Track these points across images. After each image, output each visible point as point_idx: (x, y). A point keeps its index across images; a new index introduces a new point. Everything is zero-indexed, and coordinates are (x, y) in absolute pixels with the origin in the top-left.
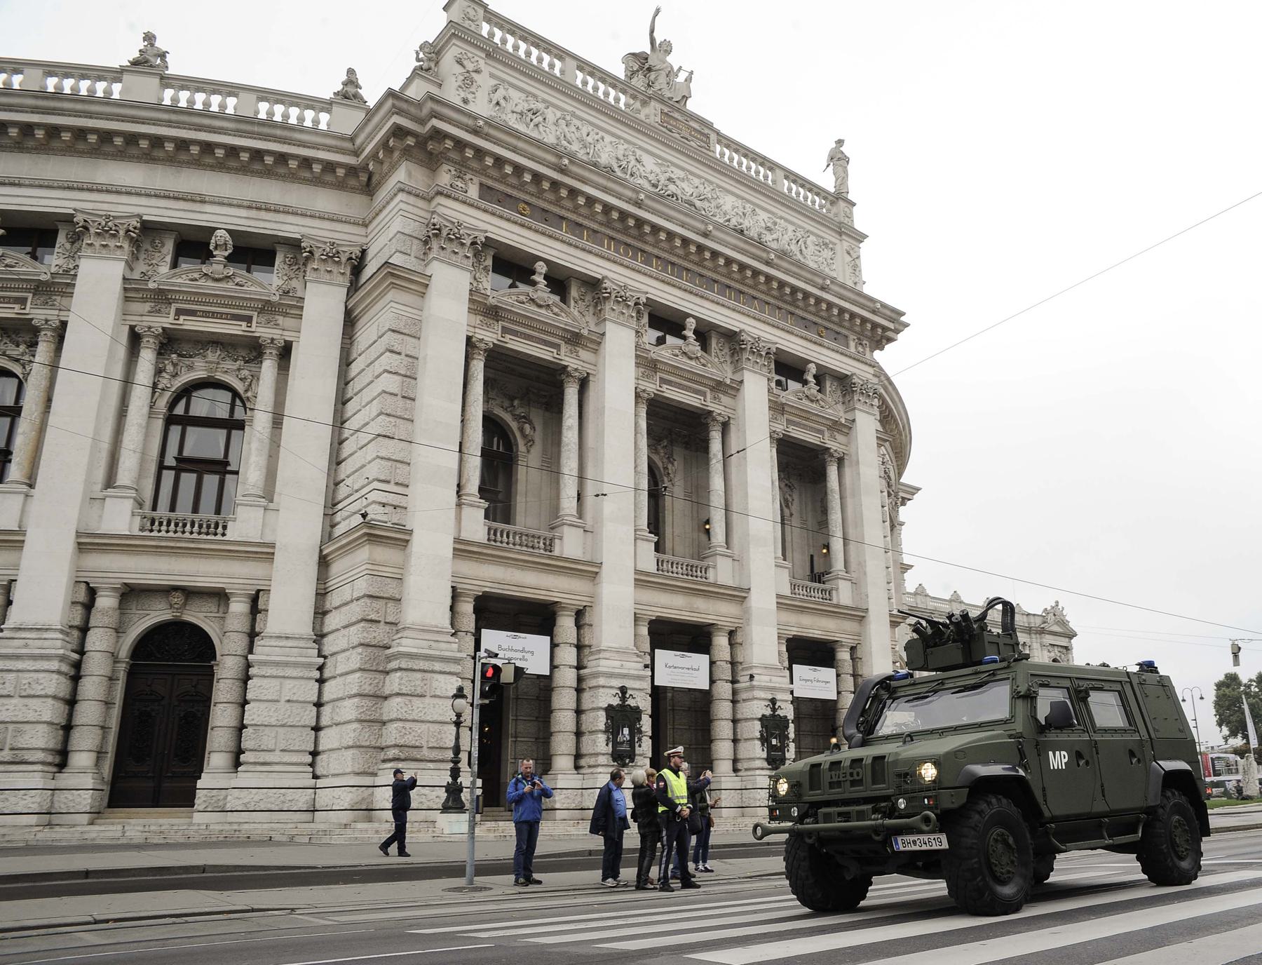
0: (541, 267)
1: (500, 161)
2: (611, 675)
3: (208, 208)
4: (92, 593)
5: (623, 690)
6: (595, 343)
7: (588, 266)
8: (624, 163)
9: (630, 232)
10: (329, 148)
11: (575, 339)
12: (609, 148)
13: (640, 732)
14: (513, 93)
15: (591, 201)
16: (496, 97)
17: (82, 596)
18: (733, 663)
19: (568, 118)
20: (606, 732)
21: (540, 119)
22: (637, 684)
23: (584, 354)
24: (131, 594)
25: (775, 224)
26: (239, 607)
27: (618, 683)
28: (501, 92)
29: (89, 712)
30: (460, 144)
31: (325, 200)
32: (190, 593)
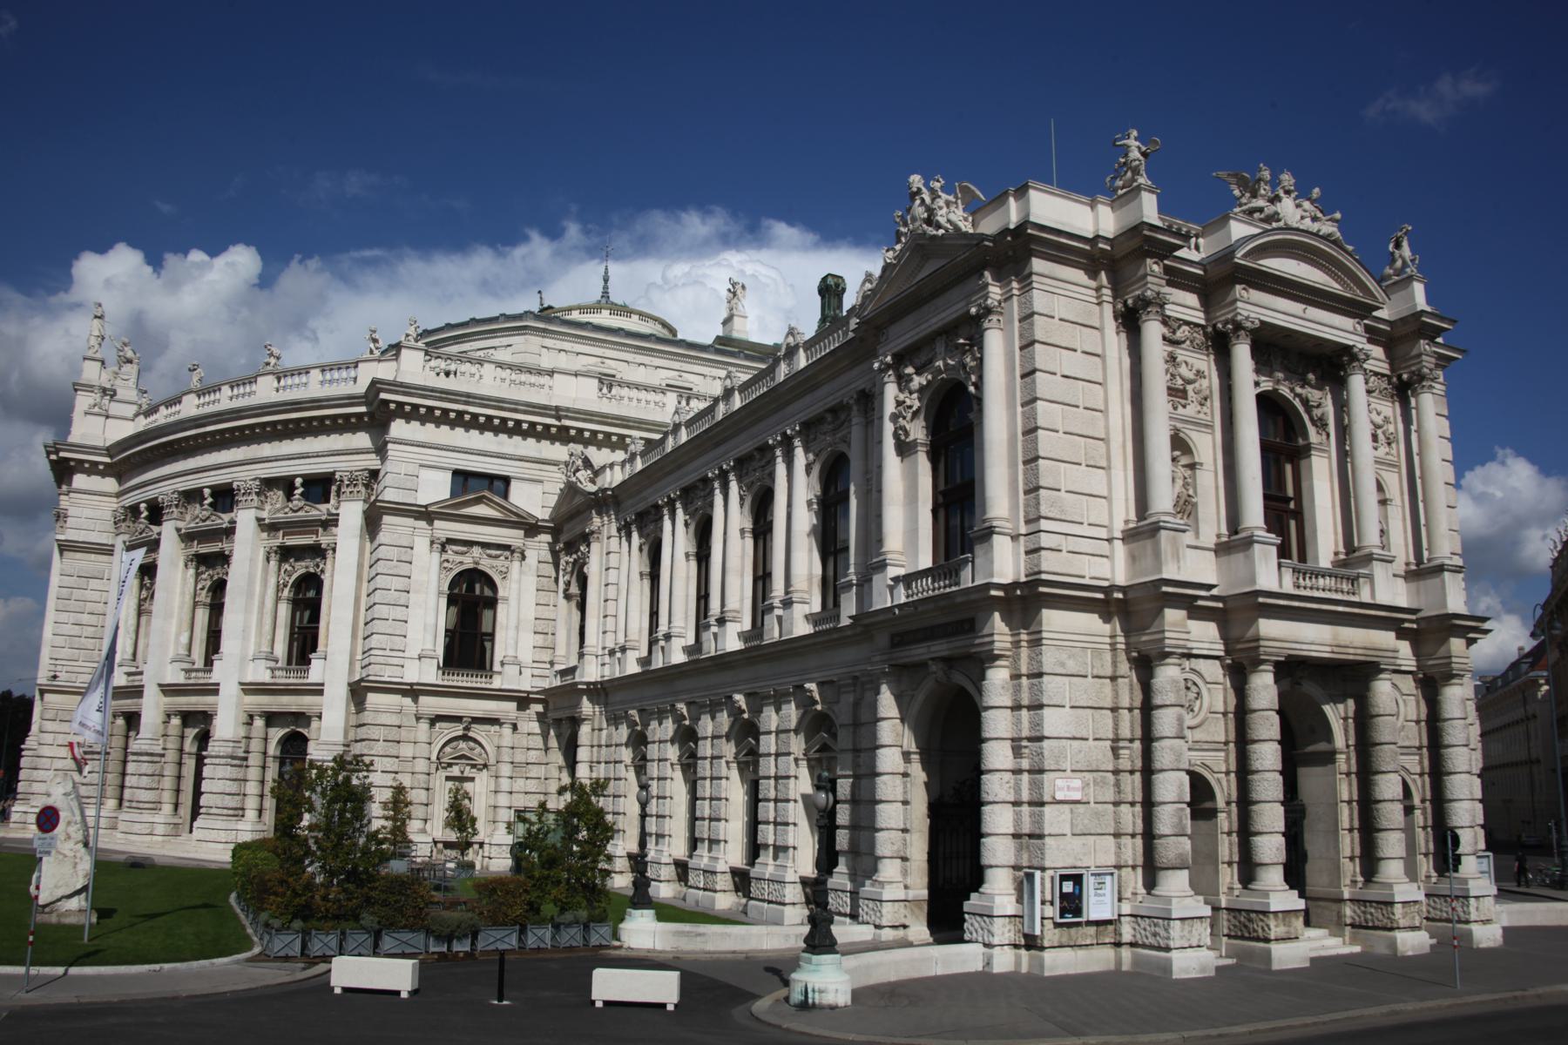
17: (244, 718)
24: (271, 719)
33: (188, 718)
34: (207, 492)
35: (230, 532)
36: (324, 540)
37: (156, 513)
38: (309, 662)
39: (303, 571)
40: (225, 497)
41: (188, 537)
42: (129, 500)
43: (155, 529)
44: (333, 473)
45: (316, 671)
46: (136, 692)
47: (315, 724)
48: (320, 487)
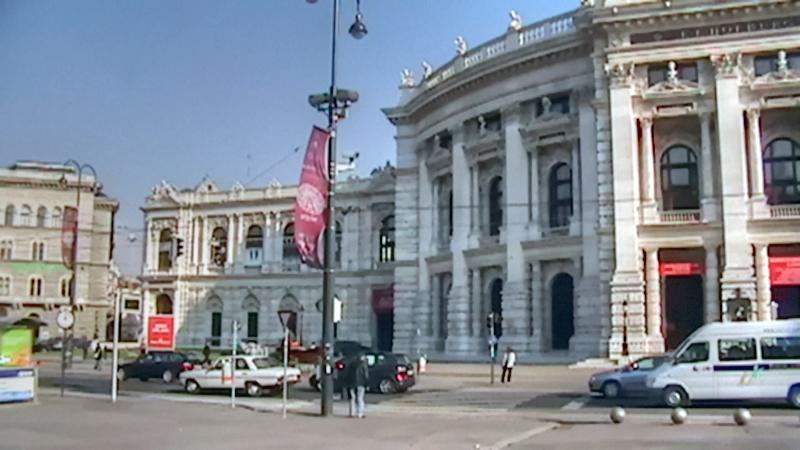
3: (541, 88)
4: (531, 266)
5: (738, 290)
10: (570, 42)
11: (699, 97)
13: (750, 311)
15: (693, 15)
20: (728, 311)
22: (748, 285)
24: (544, 264)
26: (577, 265)
29: (536, 314)
31: (580, 65)
32: (563, 261)
33: (483, 271)
34: (481, 119)
35: (502, 143)
36: (569, 137)
37: (446, 139)
38: (566, 223)
39: (555, 162)
40: (494, 119)
41: (467, 152)
42: (427, 134)
43: (446, 153)
44: (570, 91)
45: (574, 227)
46: (449, 257)
47: (577, 265)
48: (561, 100)
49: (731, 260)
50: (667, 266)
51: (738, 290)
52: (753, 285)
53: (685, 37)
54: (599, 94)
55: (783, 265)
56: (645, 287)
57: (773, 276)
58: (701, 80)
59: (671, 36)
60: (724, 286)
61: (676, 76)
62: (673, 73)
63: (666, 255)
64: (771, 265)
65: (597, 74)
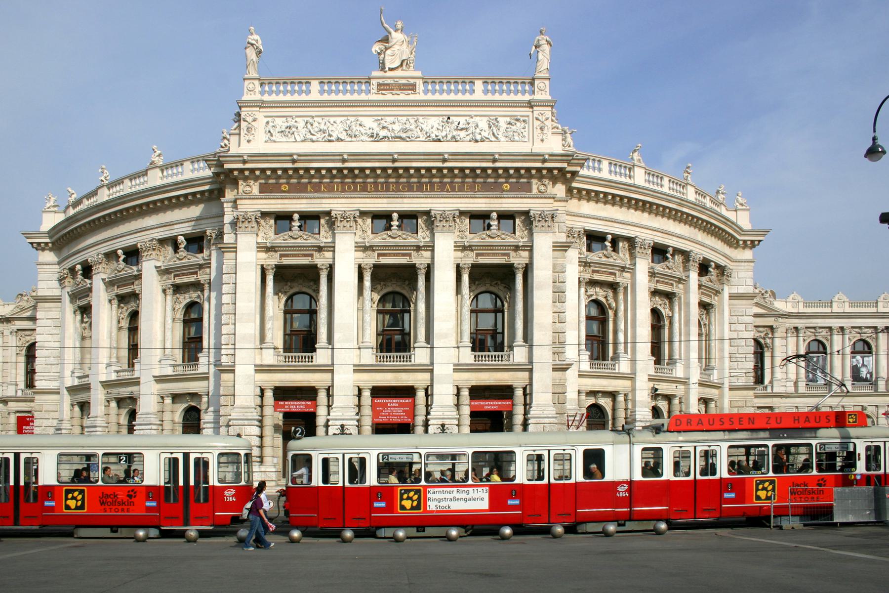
0: (296, 216)
1: (263, 170)
2: (336, 419)
6: (332, 248)
7: (324, 206)
8: (349, 132)
9: (349, 176)
11: (320, 249)
12: (340, 125)
14: (279, 121)
16: (267, 130)
18: (427, 406)
19: (311, 120)
21: (294, 129)
22: (352, 422)
23: (329, 255)
25: (468, 124)
27: (339, 423)
28: (271, 124)
30: (241, 171)
49: (337, 401)
50: (282, 403)
51: (342, 426)
52: (356, 423)
53: (311, 192)
54: (228, 238)
55: (385, 405)
56: (261, 421)
57: (375, 413)
58: (322, 233)
59: (299, 189)
60: (330, 423)
61: (300, 227)
62: (296, 224)
63: (282, 393)
64: (373, 406)
65: (228, 219)
